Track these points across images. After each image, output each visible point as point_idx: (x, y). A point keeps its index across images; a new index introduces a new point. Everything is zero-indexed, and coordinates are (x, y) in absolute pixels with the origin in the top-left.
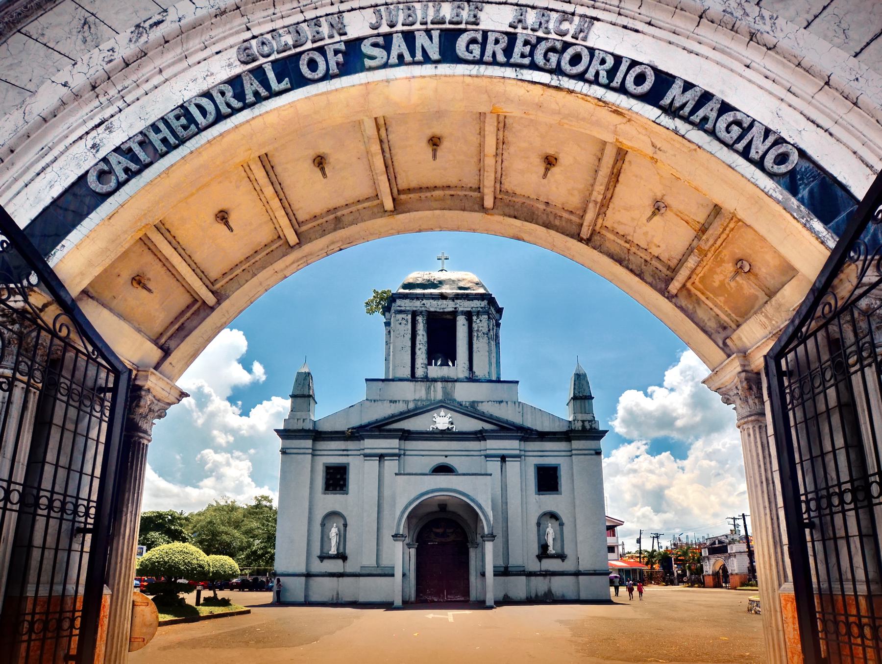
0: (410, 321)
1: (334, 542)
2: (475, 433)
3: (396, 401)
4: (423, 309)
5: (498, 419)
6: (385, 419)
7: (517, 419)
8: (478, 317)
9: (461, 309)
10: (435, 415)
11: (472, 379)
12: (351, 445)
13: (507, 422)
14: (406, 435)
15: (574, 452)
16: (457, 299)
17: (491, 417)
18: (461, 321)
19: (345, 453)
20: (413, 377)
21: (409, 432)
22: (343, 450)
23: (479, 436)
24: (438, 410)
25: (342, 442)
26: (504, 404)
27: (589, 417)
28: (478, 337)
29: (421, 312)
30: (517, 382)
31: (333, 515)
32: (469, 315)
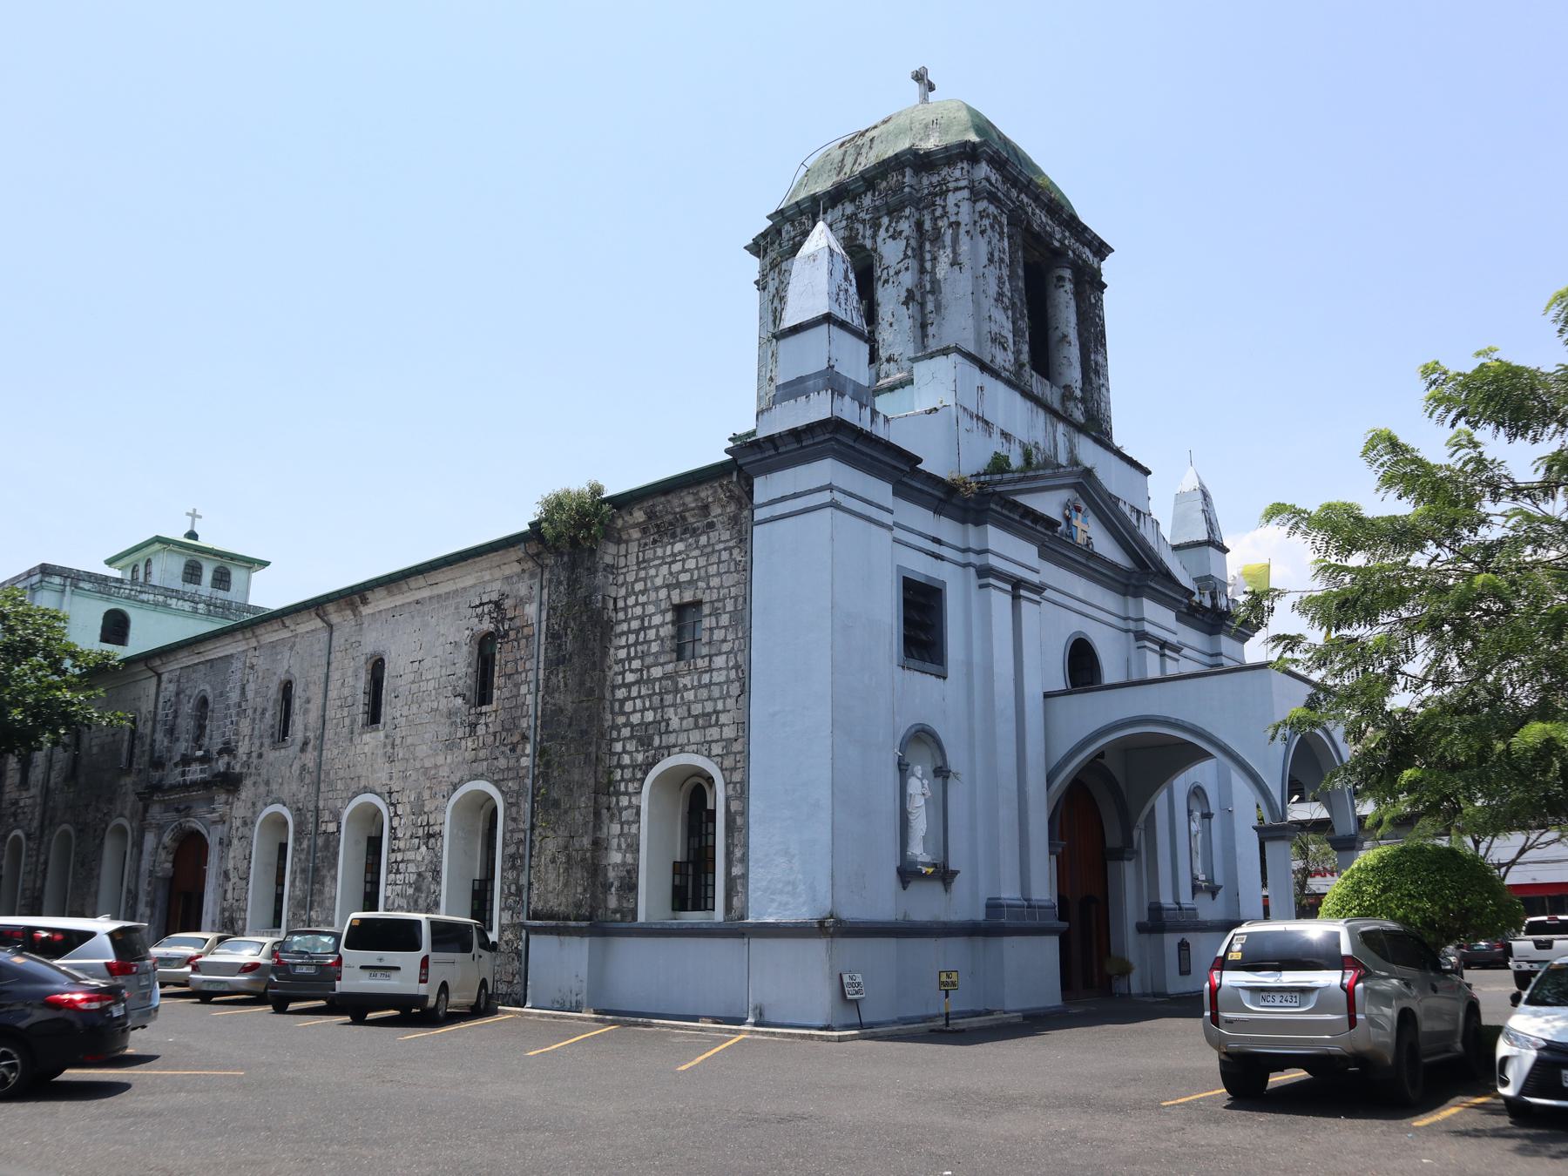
1: (920, 824)
12: (947, 529)
30: (1147, 472)
31: (922, 737)
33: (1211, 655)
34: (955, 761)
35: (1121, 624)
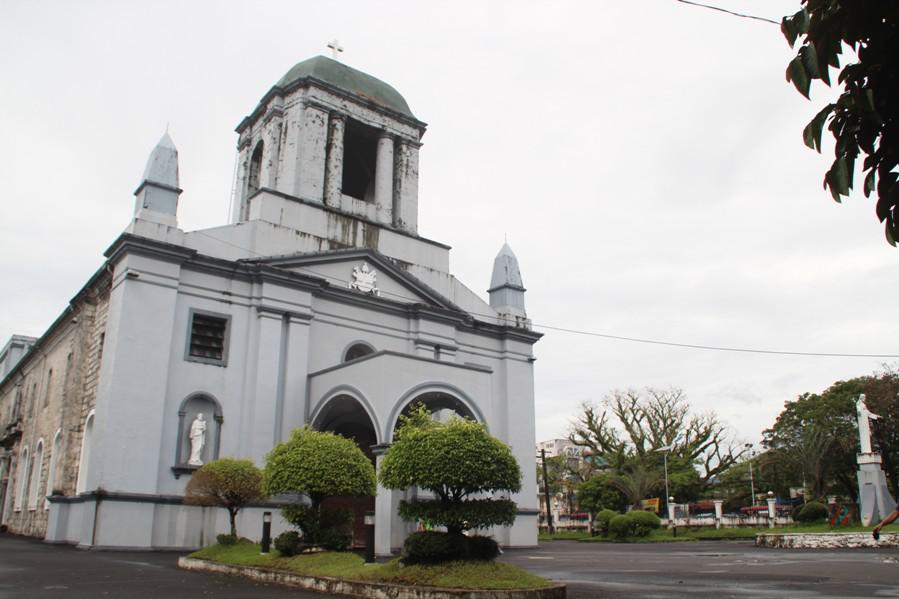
0: (326, 122)
1: (197, 445)
2: (407, 306)
3: (305, 234)
4: (343, 112)
5: (432, 293)
6: (294, 258)
7: (448, 296)
8: (408, 149)
9: (389, 130)
10: (357, 268)
11: (397, 228)
12: (238, 287)
13: (441, 299)
14: (322, 290)
15: (508, 354)
16: (386, 115)
17: (425, 288)
18: (386, 149)
19: (226, 297)
20: (324, 207)
21: (324, 283)
22: (224, 293)
23: (410, 312)
24: (360, 262)
25: (223, 280)
26: (434, 273)
27: (522, 315)
28: (407, 174)
29: (342, 116)
30: (449, 248)
31: (202, 400)
32: (397, 141)
33: (502, 352)
34: (226, 414)
35: (404, 335)
